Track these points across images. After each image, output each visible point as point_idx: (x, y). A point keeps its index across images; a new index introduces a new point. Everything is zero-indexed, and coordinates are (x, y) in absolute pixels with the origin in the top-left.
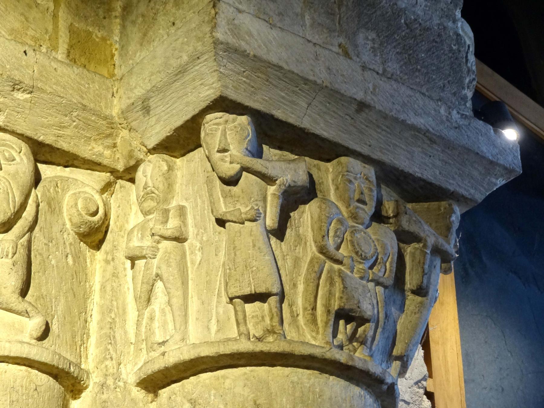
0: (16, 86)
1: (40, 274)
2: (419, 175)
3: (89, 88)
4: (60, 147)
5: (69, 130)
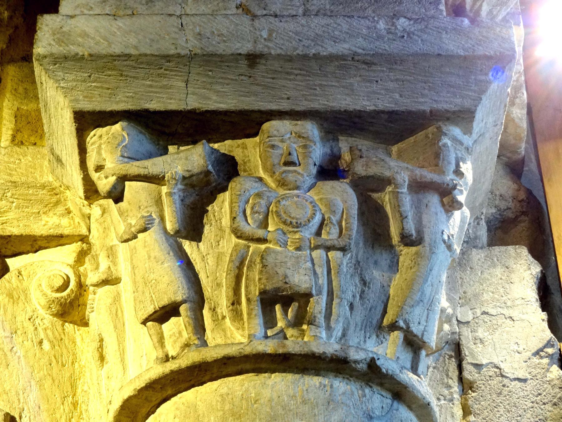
2: (372, 108)
4: (9, 234)
5: (12, 213)
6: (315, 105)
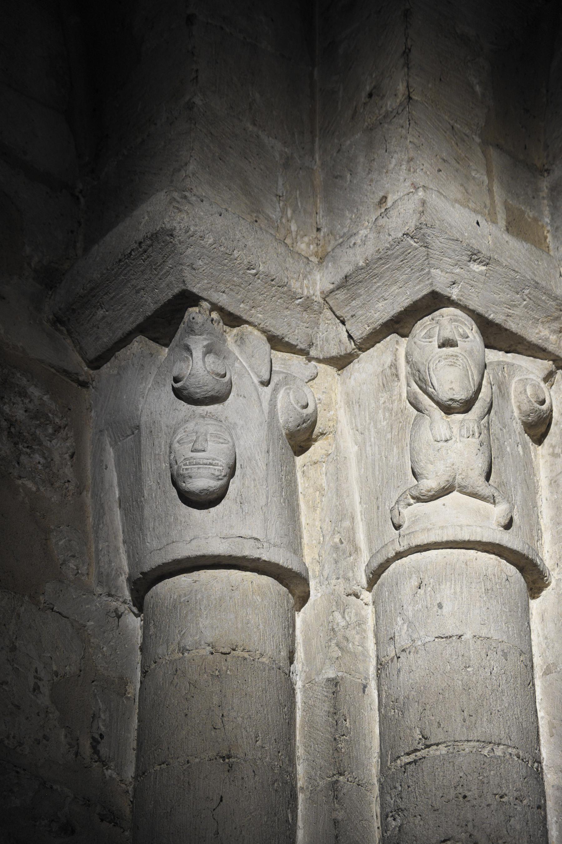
0: (473, 257)
1: (499, 460)
3: (538, 265)
4: (508, 328)
5: (519, 310)
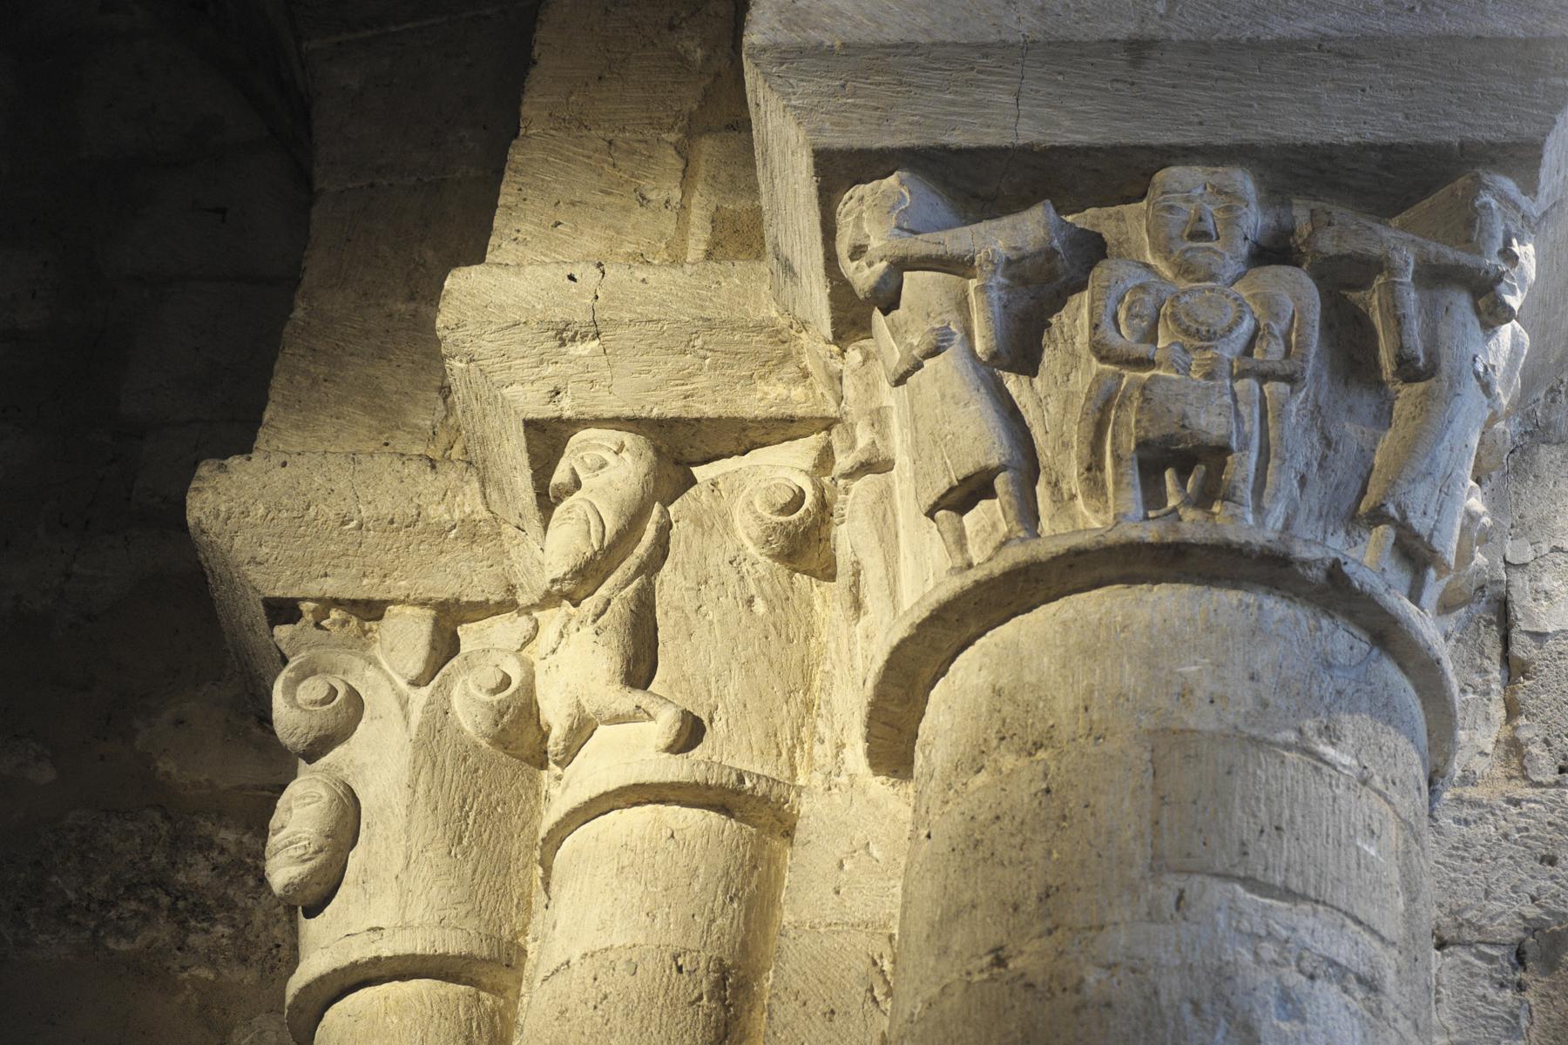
5: (702, 378)
6: (1251, 136)
